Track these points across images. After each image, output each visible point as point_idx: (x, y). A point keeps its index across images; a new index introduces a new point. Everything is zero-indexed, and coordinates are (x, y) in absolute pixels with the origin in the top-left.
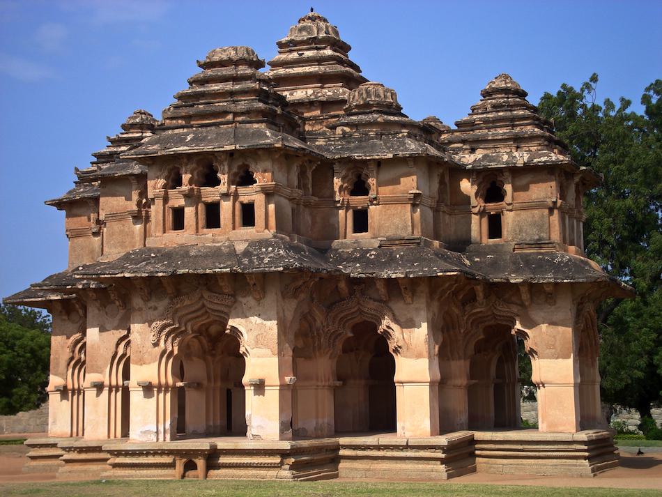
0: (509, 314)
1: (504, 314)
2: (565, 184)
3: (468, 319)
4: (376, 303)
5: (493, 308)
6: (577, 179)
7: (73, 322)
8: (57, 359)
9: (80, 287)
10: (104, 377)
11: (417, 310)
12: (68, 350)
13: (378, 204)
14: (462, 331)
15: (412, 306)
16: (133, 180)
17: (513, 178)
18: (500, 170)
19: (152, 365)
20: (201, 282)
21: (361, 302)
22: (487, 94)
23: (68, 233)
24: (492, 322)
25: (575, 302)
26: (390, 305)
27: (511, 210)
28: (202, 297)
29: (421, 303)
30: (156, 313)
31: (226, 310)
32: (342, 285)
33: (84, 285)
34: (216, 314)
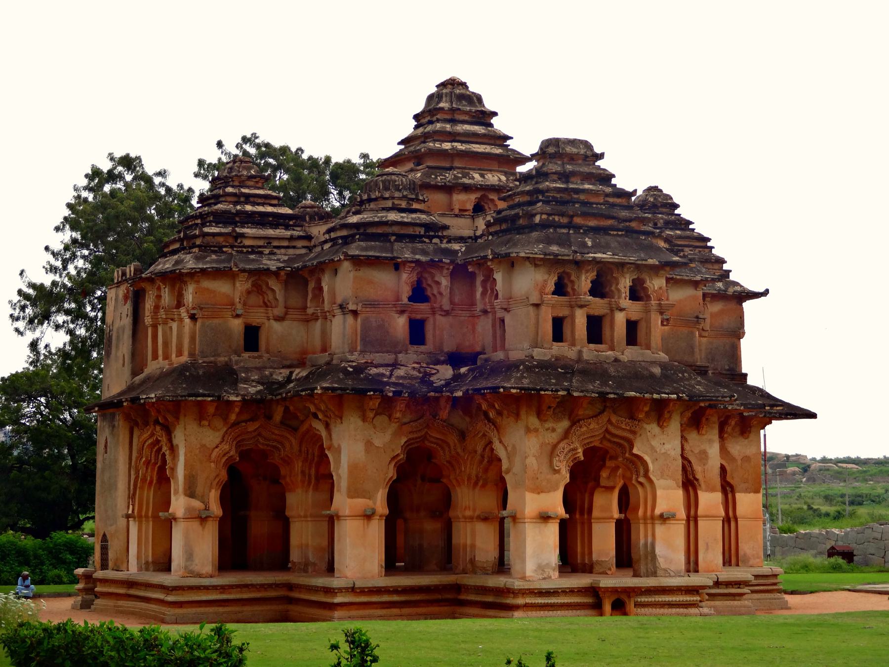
7: (215, 429)
8: (193, 476)
9: (391, 394)
10: (375, 503)
11: (710, 441)
12: (213, 465)
15: (705, 437)
16: (410, 267)
19: (552, 494)
20: (608, 405)
23: (193, 312)
28: (609, 421)
30: (554, 435)
31: (630, 436)
33: (394, 392)
34: (615, 440)
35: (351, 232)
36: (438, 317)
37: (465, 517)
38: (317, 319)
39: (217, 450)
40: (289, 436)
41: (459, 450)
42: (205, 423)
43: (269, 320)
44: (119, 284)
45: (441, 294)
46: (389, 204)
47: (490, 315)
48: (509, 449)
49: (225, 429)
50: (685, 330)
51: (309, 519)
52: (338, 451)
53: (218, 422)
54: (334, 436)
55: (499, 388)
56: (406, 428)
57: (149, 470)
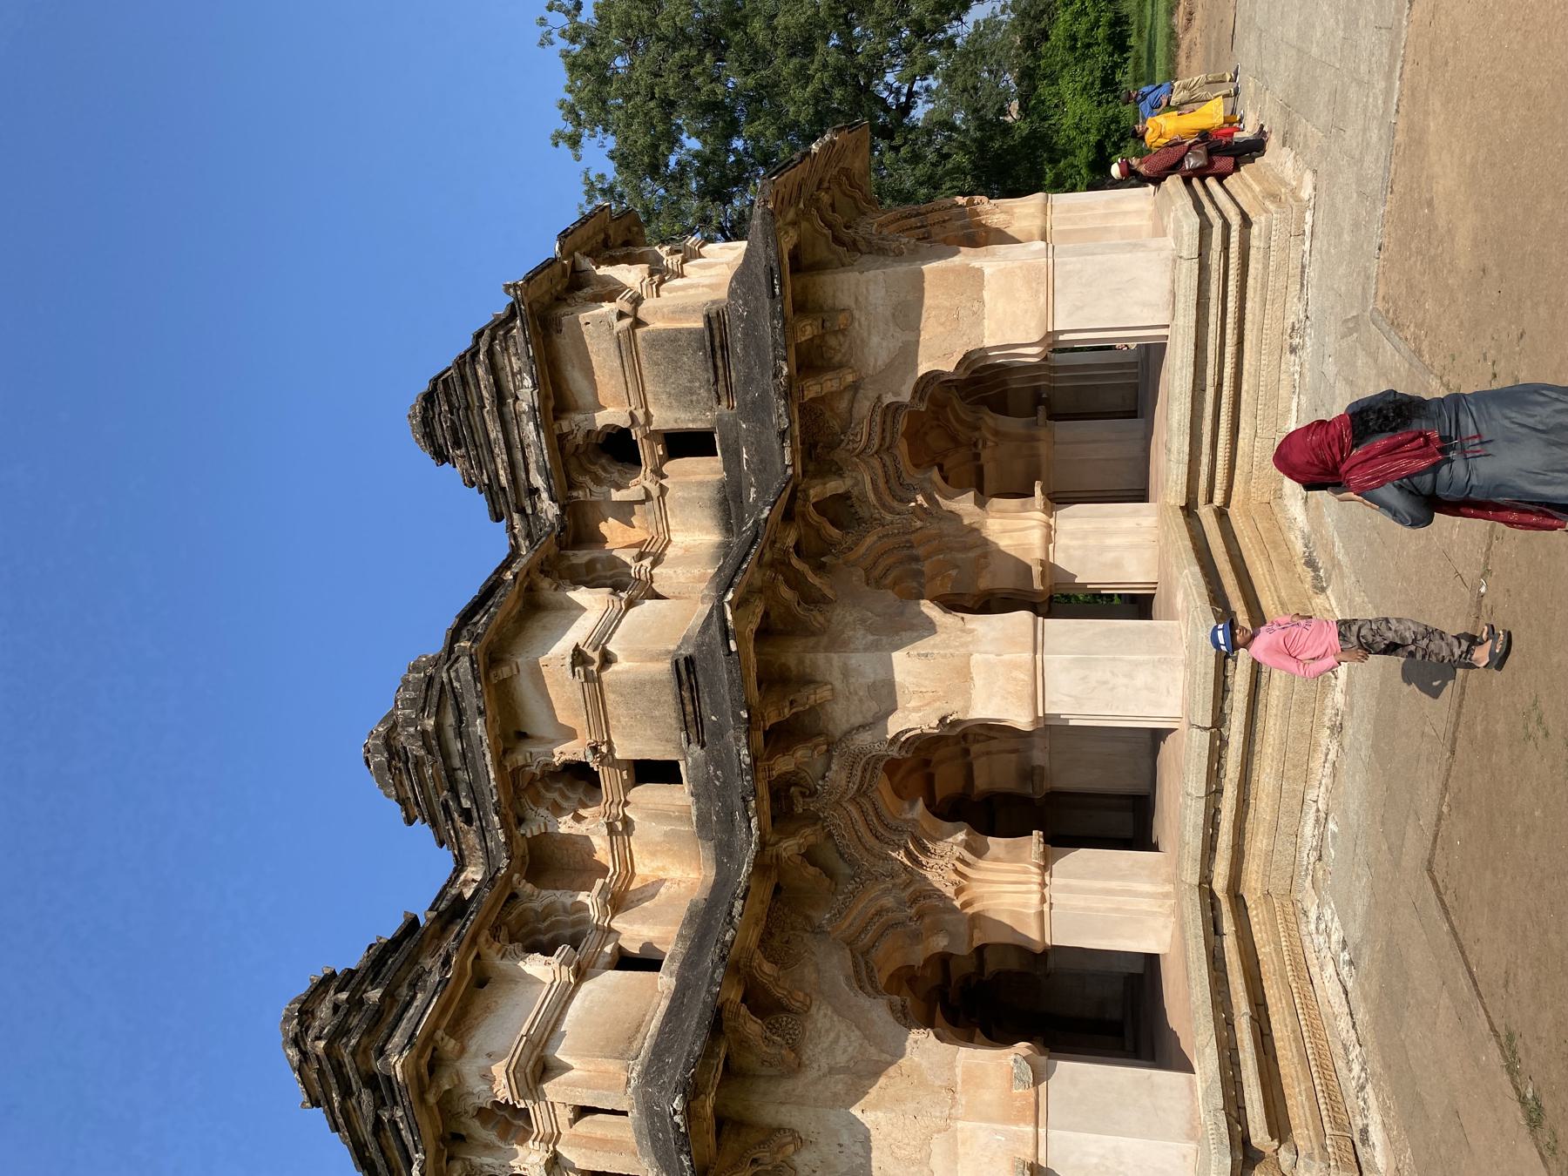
0: (878, 419)
1: (877, 429)
2: (597, 289)
3: (892, 511)
4: (834, 767)
5: (863, 456)
6: (587, 263)
11: (846, 673)
13: (609, 743)
14: (919, 524)
15: (838, 685)
17: (577, 409)
18: (559, 443)
21: (834, 798)
22: (441, 456)
24: (903, 447)
25: (847, 260)
26: (838, 734)
27: (647, 414)
29: (829, 664)
32: (789, 847)
50: (610, 697)
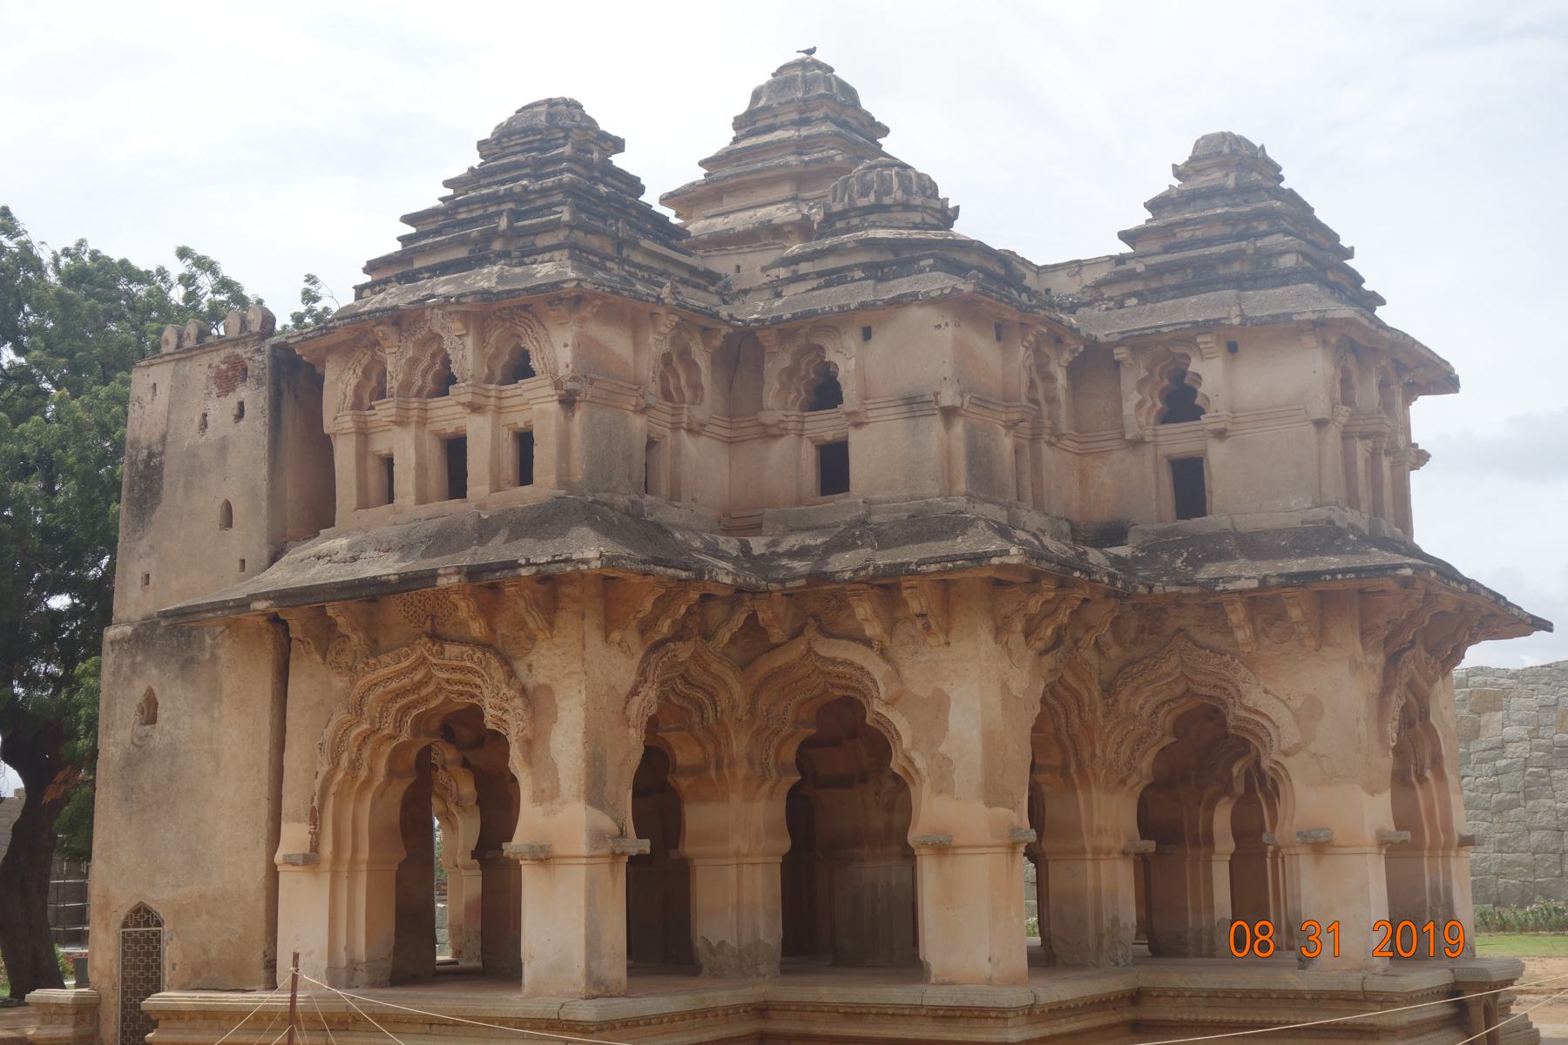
23: (577, 386)
35: (880, 258)
36: (1044, 446)
37: (1097, 851)
38: (776, 437)
39: (637, 699)
40: (730, 677)
41: (1099, 714)
42: (616, 636)
43: (675, 428)
44: (182, 354)
45: (1052, 400)
46: (916, 217)
47: (1150, 448)
48: (1297, 703)
49: (641, 654)
51: (760, 860)
52: (940, 704)
53: (633, 639)
54: (906, 673)
55: (1402, 566)
56: (1048, 661)
57: (366, 754)
